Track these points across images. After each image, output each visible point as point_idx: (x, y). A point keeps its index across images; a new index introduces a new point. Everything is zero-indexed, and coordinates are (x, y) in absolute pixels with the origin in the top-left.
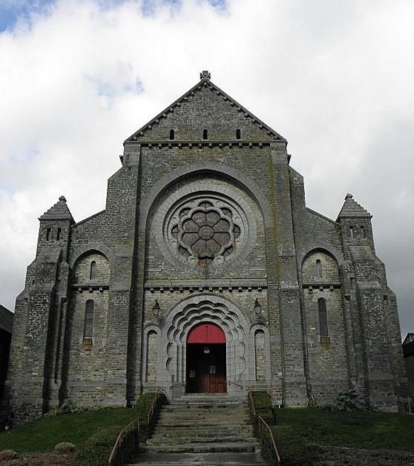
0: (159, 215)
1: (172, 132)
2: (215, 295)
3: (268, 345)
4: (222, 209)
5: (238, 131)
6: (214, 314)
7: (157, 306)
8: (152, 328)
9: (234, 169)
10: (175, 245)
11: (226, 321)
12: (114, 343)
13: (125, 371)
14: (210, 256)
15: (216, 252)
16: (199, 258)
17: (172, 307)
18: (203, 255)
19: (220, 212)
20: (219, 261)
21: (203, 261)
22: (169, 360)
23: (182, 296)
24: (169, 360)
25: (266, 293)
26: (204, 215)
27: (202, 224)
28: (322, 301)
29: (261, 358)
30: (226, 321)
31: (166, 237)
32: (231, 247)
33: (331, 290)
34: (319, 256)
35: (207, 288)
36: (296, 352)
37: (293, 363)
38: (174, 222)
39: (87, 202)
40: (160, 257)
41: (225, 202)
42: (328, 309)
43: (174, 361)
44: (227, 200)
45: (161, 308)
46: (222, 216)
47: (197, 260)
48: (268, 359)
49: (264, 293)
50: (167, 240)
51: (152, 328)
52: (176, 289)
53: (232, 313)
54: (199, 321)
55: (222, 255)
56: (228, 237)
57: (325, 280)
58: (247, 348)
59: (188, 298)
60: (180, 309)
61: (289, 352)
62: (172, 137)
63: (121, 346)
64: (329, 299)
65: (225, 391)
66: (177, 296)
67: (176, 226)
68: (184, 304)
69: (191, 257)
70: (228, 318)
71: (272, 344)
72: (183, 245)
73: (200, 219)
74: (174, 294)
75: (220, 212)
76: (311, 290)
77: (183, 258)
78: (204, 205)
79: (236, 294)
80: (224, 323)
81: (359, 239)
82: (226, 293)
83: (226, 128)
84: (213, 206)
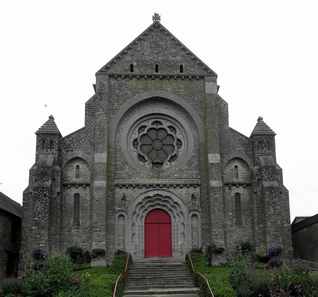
0: (124, 131)
1: (132, 66)
2: (164, 190)
3: (200, 225)
4: (169, 127)
5: (181, 66)
6: (163, 204)
7: (124, 198)
8: (121, 213)
9: (178, 97)
10: (135, 154)
12: (96, 224)
13: (104, 243)
14: (160, 161)
15: (164, 159)
16: (153, 164)
18: (155, 161)
19: (168, 129)
20: (166, 166)
21: (156, 165)
22: (133, 234)
24: (133, 234)
26: (156, 131)
27: (155, 139)
28: (238, 195)
29: (195, 233)
31: (129, 148)
32: (175, 155)
33: (244, 187)
34: (237, 163)
35: (158, 185)
36: (220, 230)
37: (217, 237)
38: (135, 136)
39: (71, 122)
40: (126, 163)
41: (171, 122)
42: (242, 200)
44: (172, 121)
45: (127, 199)
46: (169, 132)
47: (151, 165)
48: (200, 234)
49: (198, 189)
50: (130, 150)
51: (121, 213)
52: (137, 185)
53: (176, 203)
55: (169, 161)
56: (173, 149)
57: (240, 180)
58: (186, 227)
59: (145, 192)
60: (140, 200)
61: (215, 230)
62: (132, 70)
63: (101, 226)
64: (243, 194)
65: (171, 255)
66: (138, 191)
67: (136, 140)
68: (143, 197)
69: (147, 163)
70: (173, 206)
71: (203, 224)
72: (141, 154)
73: (153, 134)
74: (136, 189)
75: (168, 129)
76: (230, 187)
77: (142, 163)
78: (156, 124)
79: (178, 191)
80: (170, 210)
81: (266, 151)
82: (172, 189)
83: (172, 63)
84: (162, 124)
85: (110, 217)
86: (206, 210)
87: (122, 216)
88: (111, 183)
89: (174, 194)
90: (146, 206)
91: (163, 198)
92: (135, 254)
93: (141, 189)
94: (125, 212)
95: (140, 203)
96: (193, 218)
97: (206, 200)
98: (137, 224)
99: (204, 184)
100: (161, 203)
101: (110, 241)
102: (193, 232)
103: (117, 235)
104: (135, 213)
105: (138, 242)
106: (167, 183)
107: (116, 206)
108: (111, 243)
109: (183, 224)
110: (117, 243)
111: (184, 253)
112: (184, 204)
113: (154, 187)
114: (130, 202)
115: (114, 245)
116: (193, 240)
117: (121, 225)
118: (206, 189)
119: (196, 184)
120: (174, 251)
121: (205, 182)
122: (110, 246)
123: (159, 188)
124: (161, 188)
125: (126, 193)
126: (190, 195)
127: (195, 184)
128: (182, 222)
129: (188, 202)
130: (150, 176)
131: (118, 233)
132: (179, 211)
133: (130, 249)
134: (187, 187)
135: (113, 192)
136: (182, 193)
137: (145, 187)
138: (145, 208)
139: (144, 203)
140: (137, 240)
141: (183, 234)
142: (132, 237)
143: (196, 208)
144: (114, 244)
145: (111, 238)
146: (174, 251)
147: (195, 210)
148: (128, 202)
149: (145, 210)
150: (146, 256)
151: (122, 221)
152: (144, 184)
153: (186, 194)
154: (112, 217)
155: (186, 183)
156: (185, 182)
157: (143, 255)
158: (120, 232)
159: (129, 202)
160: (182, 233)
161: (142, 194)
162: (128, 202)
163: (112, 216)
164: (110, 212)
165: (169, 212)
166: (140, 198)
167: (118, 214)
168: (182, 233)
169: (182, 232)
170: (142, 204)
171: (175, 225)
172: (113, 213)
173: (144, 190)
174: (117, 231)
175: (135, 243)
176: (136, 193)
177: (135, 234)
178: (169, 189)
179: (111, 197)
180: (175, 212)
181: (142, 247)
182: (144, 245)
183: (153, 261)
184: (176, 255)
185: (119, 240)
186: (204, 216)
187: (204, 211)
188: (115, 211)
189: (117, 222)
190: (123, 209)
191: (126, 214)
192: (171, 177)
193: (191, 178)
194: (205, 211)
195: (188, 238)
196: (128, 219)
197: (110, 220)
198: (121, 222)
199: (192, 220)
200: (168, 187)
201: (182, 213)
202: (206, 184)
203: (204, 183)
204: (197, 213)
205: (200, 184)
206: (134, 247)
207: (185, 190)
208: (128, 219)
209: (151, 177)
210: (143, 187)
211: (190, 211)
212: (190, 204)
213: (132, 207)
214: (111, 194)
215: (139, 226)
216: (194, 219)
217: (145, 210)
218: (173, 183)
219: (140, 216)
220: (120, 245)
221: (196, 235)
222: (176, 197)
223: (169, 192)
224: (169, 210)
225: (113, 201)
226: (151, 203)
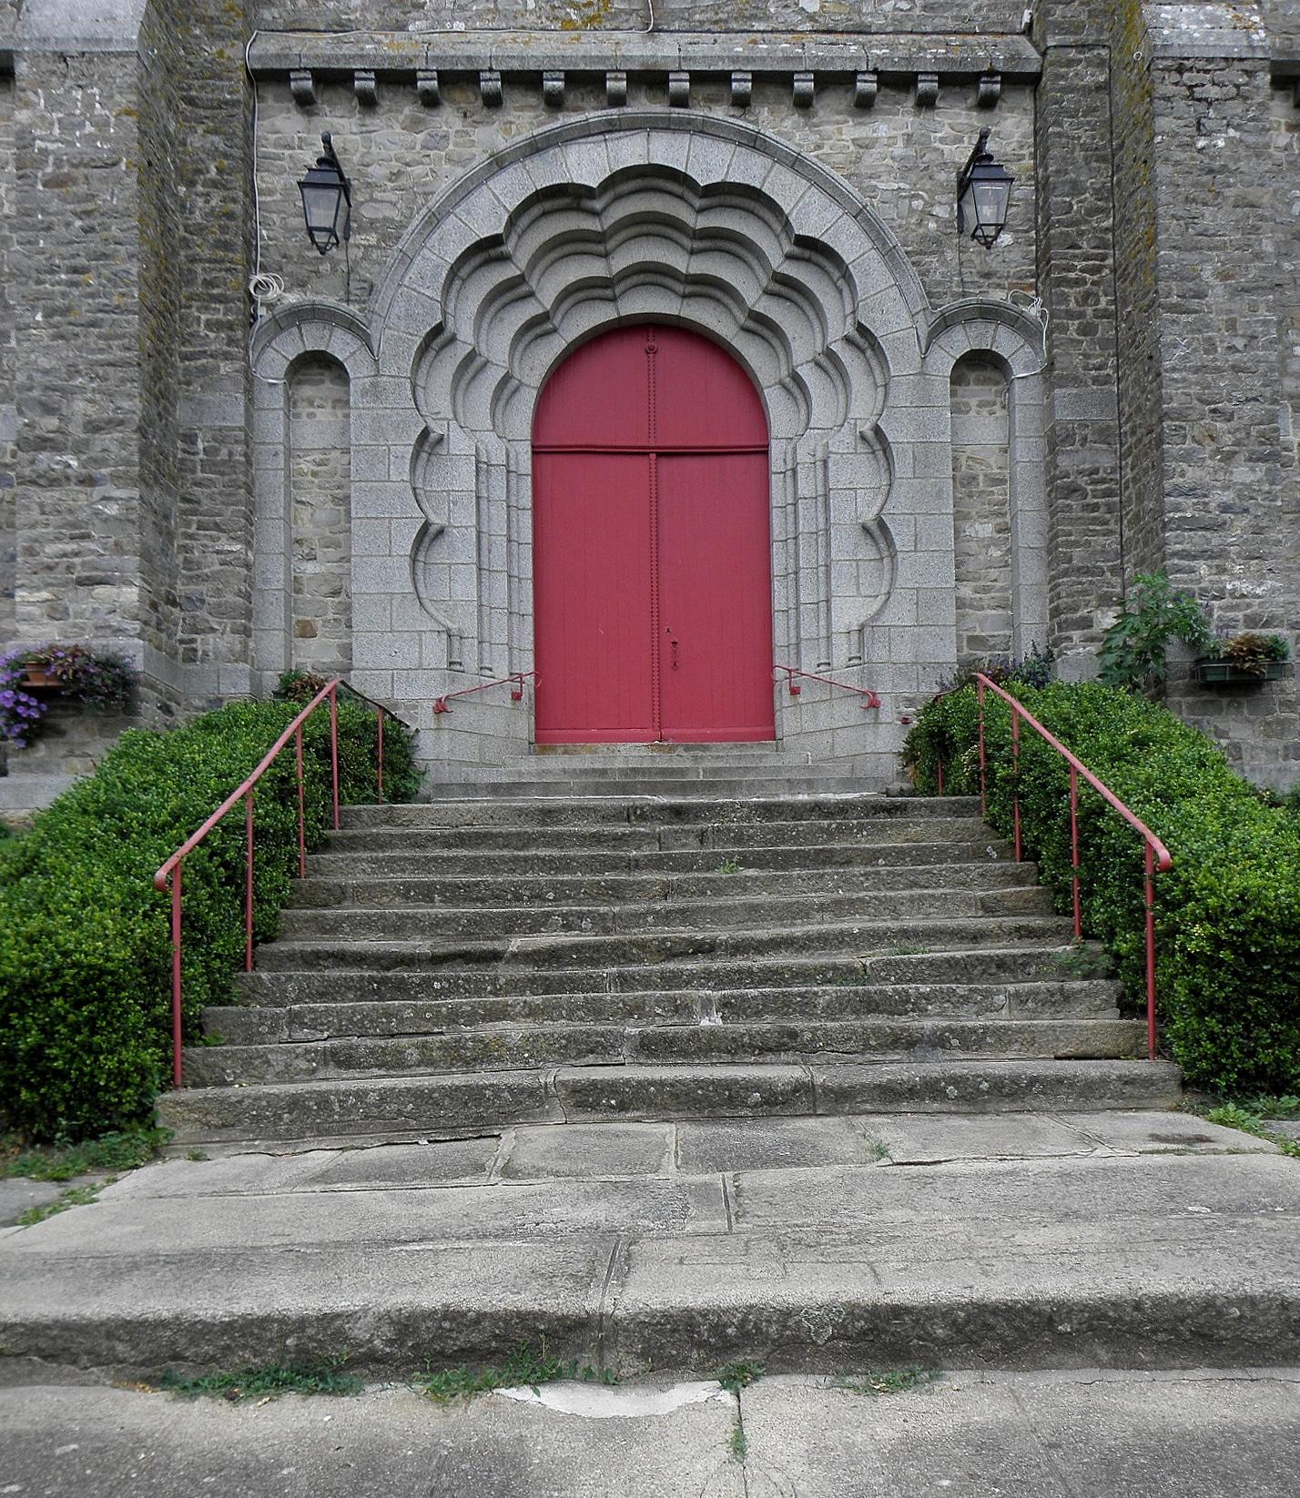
2: (703, 129)
3: (1028, 452)
6: (699, 266)
7: (330, 173)
8: (313, 338)
11: (774, 310)
12: (49, 410)
13: (130, 595)
17: (434, 201)
22: (428, 536)
23: (498, 134)
24: (428, 536)
25: (1027, 125)
29: (985, 529)
30: (774, 310)
35: (650, 80)
36: (1243, 473)
37: (1215, 539)
43: (459, 550)
48: (1030, 531)
51: (313, 338)
52: (458, 80)
53: (812, 250)
54: (599, 315)
58: (903, 467)
59: (536, 147)
60: (484, 216)
61: (1193, 474)
63: (94, 427)
65: (764, 727)
66: (465, 137)
68: (514, 187)
70: (785, 287)
71: (1055, 441)
74: (448, 120)
79: (834, 135)
80: (761, 326)
82: (775, 122)
85: (204, 371)
86: (1089, 310)
87: (317, 364)
88: (210, 50)
89: (795, 163)
90: (548, 290)
91: (700, 211)
92: (440, 709)
93: (499, 118)
94: (351, 325)
95: (487, 250)
96: (960, 389)
97: (1092, 212)
98: (460, 443)
99: (1070, 63)
100: (680, 262)
101: (203, 588)
102: (966, 517)
103: (273, 536)
104: (437, 338)
105: (473, 608)
106: (735, 59)
107: (264, 269)
108: (219, 611)
109: (878, 442)
110: (273, 614)
111: (886, 702)
112: (888, 254)
113: (618, 100)
114: (389, 232)
115: (246, 632)
116: (966, 591)
117: (318, 457)
118: (1091, 110)
119: (1000, 67)
120: (795, 691)
121: (1082, 47)
122: (210, 637)
123: (659, 109)
124: (678, 112)
125: (356, 159)
126: (942, 176)
127: (991, 73)
128: (866, 428)
129: (924, 238)
130: (576, 7)
131: (289, 521)
132: (838, 327)
133: (395, 665)
134: (910, 102)
135: (229, 137)
136: (870, 159)
137: (533, 100)
138: (529, 310)
139: (522, 251)
140: (464, 587)
141: (878, 532)
142: (414, 561)
143: (998, 296)
144: (246, 620)
145: (213, 564)
146: (795, 691)
147: (989, 313)
148: (373, 239)
149: (538, 327)
150: (544, 738)
151: (324, 415)
152: (516, 65)
153: (905, 169)
154: (225, 368)
155: (908, 59)
156: (902, 52)
157: (524, 726)
158: (305, 513)
159: (384, 237)
160: (865, 529)
161: (499, 163)
162: (373, 239)
163: (227, 356)
164: (208, 324)
165: (753, 353)
167: (289, 347)
168: (865, 529)
169: (869, 516)
170: (505, 258)
171: (802, 455)
172: (230, 326)
173: (523, 120)
174: (274, 503)
175: (440, 618)
176: (449, 160)
177: (441, 532)
178: (755, 122)
179: (214, 184)
180: (803, 345)
181: (510, 650)
182: (528, 641)
183: (603, 772)
184: (809, 727)
185: (296, 585)
186: (1078, 360)
187: (1070, 315)
188: (254, 317)
189: (272, 424)
190: (331, 301)
191: (355, 344)
192: (767, 18)
193: (951, 25)
194: (1081, 315)
195: (925, 568)
196: (375, 391)
197: (208, 397)
198: (318, 424)
199: (956, 409)
200: (742, 102)
201: (864, 339)
202: (1089, 63)
203: (1073, 54)
204: (1005, 342)
205: (1034, 68)
206: (435, 652)
207: (893, 126)
208: (375, 391)
209: (591, 12)
210: (514, 99)
211: (944, 324)
212: (944, 263)
213: (414, 289)
214: (214, 153)
215: (482, 468)
216: (974, 402)
217: (538, 327)
218: (787, 59)
219: (492, 377)
220: (307, 631)
221: (994, 542)
222: (816, 198)
223: (755, 143)
224: (745, 329)
225: (230, 216)
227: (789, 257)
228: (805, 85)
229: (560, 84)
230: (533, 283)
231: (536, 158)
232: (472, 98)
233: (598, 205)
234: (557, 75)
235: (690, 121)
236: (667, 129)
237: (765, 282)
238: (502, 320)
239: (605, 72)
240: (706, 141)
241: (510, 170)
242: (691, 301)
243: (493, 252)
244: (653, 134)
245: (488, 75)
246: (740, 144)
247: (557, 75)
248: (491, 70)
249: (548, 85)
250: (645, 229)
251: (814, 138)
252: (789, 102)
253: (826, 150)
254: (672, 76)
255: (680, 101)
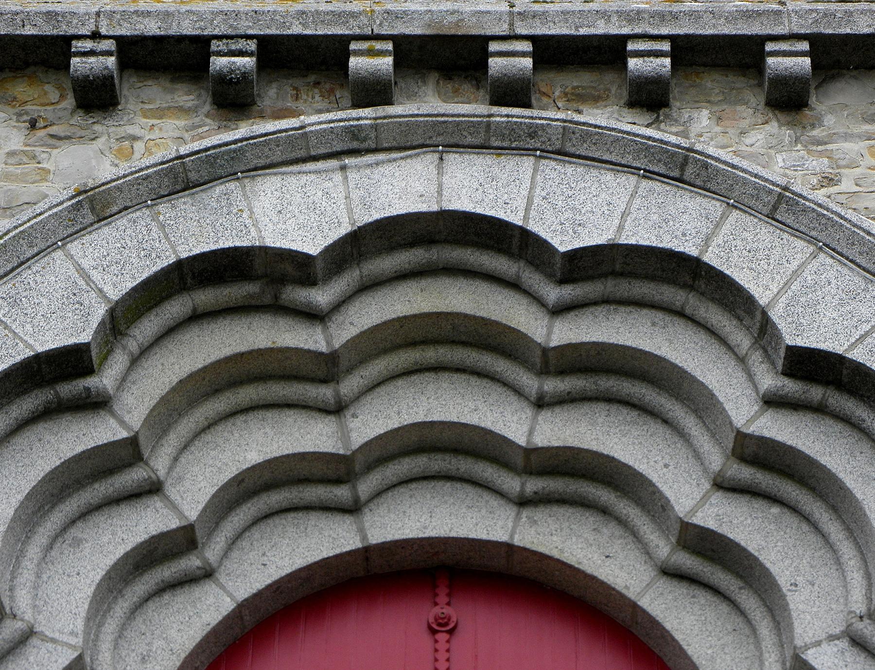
2: (562, 148)
6: (557, 431)
54: (322, 540)
70: (767, 471)
80: (711, 562)
82: (723, 131)
89: (779, 207)
90: (196, 480)
91: (559, 311)
93: (107, 130)
123: (471, 108)
137: (185, 96)
138: (147, 522)
139: (137, 392)
161: (96, 206)
166: (53, 275)
170: (96, 404)
173: (162, 128)
178: (685, 135)
200: (650, 98)
217: (165, 563)
222: (831, 275)
223: (683, 170)
226: (291, 419)
227: (773, 402)
228: (794, 63)
229: (247, 62)
230: (160, 463)
231: (184, 203)
232: (54, 95)
233: (321, 297)
234: (241, 44)
235: (533, 132)
236: (482, 147)
237: (716, 459)
238: (77, 543)
239: (345, 40)
240: (571, 170)
241: (122, 222)
242: (540, 514)
243: (67, 389)
244: (452, 158)
245: (88, 45)
246: (649, 174)
247: (241, 44)
248: (96, 36)
249: (219, 63)
250: (431, 355)
251: (819, 164)
252: (757, 99)
253: (847, 185)
254: (493, 47)
255: (512, 93)
